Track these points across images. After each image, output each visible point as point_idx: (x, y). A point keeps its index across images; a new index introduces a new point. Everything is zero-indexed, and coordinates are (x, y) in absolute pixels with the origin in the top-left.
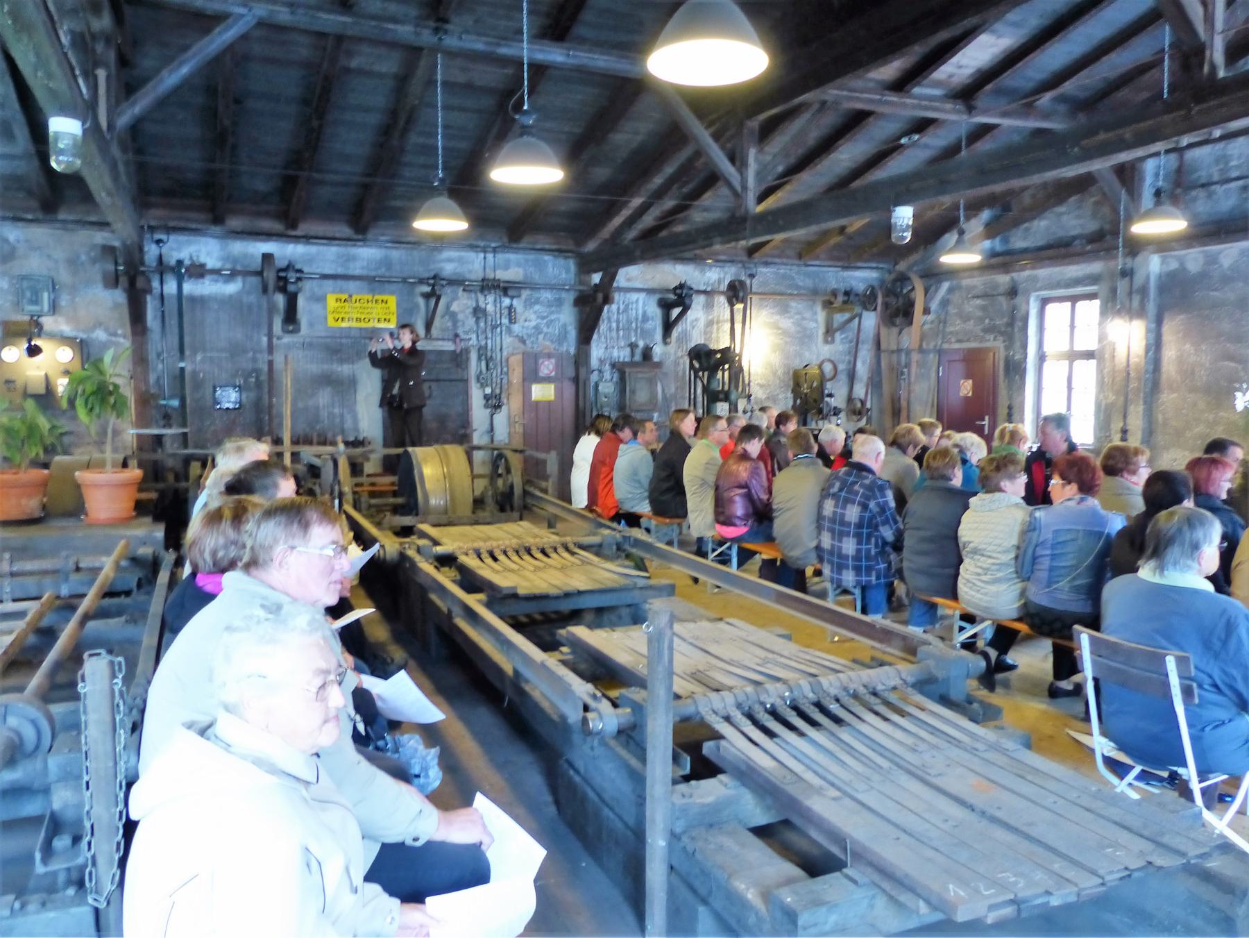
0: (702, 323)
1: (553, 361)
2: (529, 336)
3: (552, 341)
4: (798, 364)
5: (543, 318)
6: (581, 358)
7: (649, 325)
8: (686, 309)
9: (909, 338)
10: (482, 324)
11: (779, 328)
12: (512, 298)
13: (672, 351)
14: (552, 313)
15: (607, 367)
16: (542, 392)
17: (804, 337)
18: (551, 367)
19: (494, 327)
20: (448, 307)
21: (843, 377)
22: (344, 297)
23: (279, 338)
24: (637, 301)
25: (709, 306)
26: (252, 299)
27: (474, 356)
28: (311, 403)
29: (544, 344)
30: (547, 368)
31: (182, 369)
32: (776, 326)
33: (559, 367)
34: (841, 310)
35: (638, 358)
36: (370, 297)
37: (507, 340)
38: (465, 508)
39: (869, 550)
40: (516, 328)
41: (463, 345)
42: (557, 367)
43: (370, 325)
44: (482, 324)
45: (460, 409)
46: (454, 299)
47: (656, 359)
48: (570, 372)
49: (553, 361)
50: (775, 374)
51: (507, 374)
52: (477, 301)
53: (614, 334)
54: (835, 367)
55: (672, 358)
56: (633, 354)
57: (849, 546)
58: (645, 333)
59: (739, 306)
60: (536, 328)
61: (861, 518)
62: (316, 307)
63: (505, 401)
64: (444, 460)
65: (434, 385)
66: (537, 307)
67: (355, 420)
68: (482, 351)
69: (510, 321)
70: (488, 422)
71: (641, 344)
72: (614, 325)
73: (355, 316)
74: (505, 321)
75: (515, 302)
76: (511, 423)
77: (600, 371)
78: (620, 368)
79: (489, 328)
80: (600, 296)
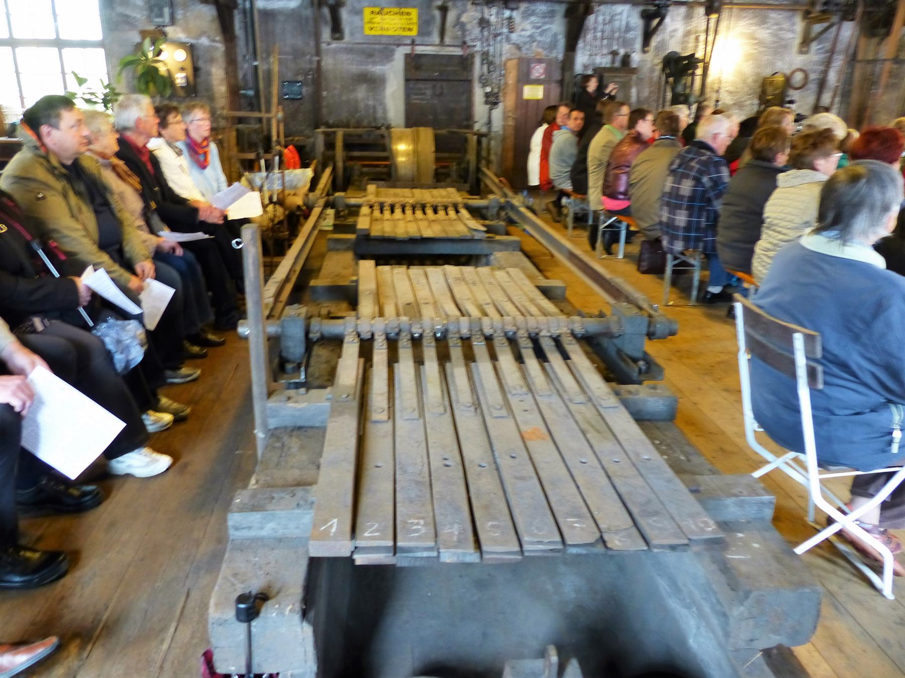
0: (680, 33)
1: (543, 65)
2: (525, 43)
3: (543, 48)
4: (767, 72)
5: (538, 28)
6: (568, 62)
7: (630, 35)
8: (663, 19)
9: (888, 49)
10: (486, 33)
11: (756, 39)
12: (512, 10)
13: (649, 59)
14: (545, 23)
16: (534, 93)
17: (779, 47)
18: (541, 71)
19: (496, 35)
20: (459, 17)
21: (813, 87)
22: (377, 10)
23: (329, 44)
24: (621, 14)
25: (688, 17)
26: (309, 12)
28: (352, 97)
29: (536, 50)
30: (538, 71)
31: (256, 67)
32: (752, 37)
33: (547, 71)
34: (820, 20)
35: (617, 64)
36: (396, 10)
37: (506, 47)
38: (429, 178)
39: (698, 222)
40: (514, 37)
41: (468, 51)
45: (464, 105)
46: (463, 12)
47: (634, 65)
48: (557, 75)
49: (543, 65)
50: (744, 81)
51: (504, 75)
52: (483, 13)
53: (598, 43)
54: (806, 77)
55: (649, 65)
56: (613, 62)
57: (681, 219)
58: (626, 43)
59: (714, 17)
60: (531, 36)
61: (694, 191)
62: (356, 19)
63: (501, 99)
64: (416, 140)
65: (445, 84)
66: (533, 18)
67: (385, 111)
70: (486, 116)
71: (622, 52)
72: (599, 34)
74: (505, 30)
75: (515, 14)
76: (505, 118)
78: (600, 73)
80: (581, 8)
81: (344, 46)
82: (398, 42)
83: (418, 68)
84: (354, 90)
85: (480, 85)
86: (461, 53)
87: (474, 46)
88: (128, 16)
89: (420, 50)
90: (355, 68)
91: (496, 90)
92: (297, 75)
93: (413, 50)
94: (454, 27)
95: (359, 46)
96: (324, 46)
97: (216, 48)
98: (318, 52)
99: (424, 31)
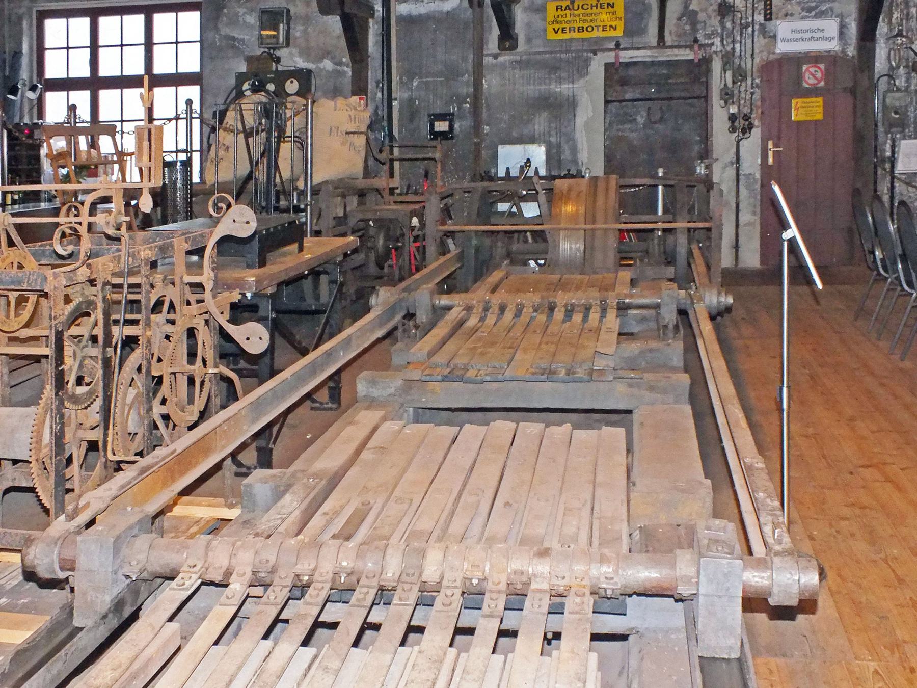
1: (822, 66)
10: (729, 25)
15: (902, 70)
18: (819, 75)
19: (744, 27)
23: (495, 56)
27: (717, 65)
42: (827, 75)
43: (595, 34)
44: (729, 25)
49: (822, 66)
62: (536, 19)
68: (728, 59)
69: (766, 19)
73: (576, 25)
74: (760, 18)
77: (890, 77)
79: (738, 28)
81: (518, 58)
82: (596, 47)
83: (624, 82)
84: (529, 121)
85: (722, 102)
86: (691, 57)
87: (713, 44)
88: (234, 39)
89: (626, 56)
90: (532, 90)
91: (746, 110)
92: (448, 103)
93: (617, 57)
94: (679, 19)
95: (538, 57)
96: (488, 60)
97: (345, 73)
98: (478, 71)
99: (633, 28)
